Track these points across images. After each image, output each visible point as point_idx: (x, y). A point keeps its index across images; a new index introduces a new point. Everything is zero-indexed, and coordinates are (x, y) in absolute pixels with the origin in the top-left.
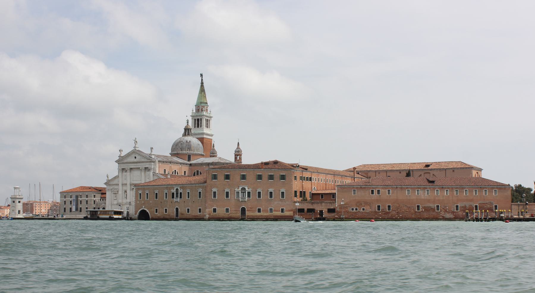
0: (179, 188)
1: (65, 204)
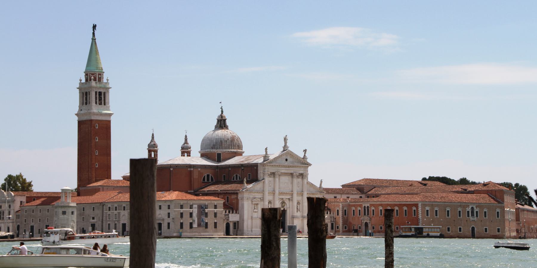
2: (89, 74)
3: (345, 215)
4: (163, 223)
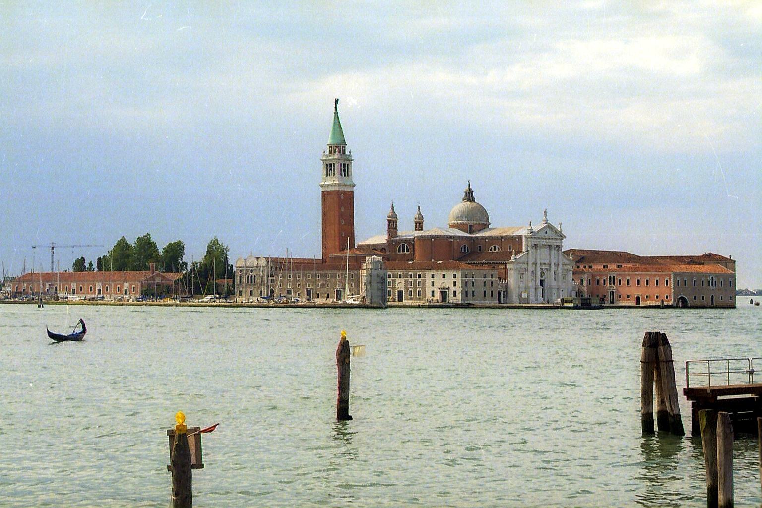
0: (714, 277)
1: (466, 286)
3: (590, 284)
4: (449, 291)
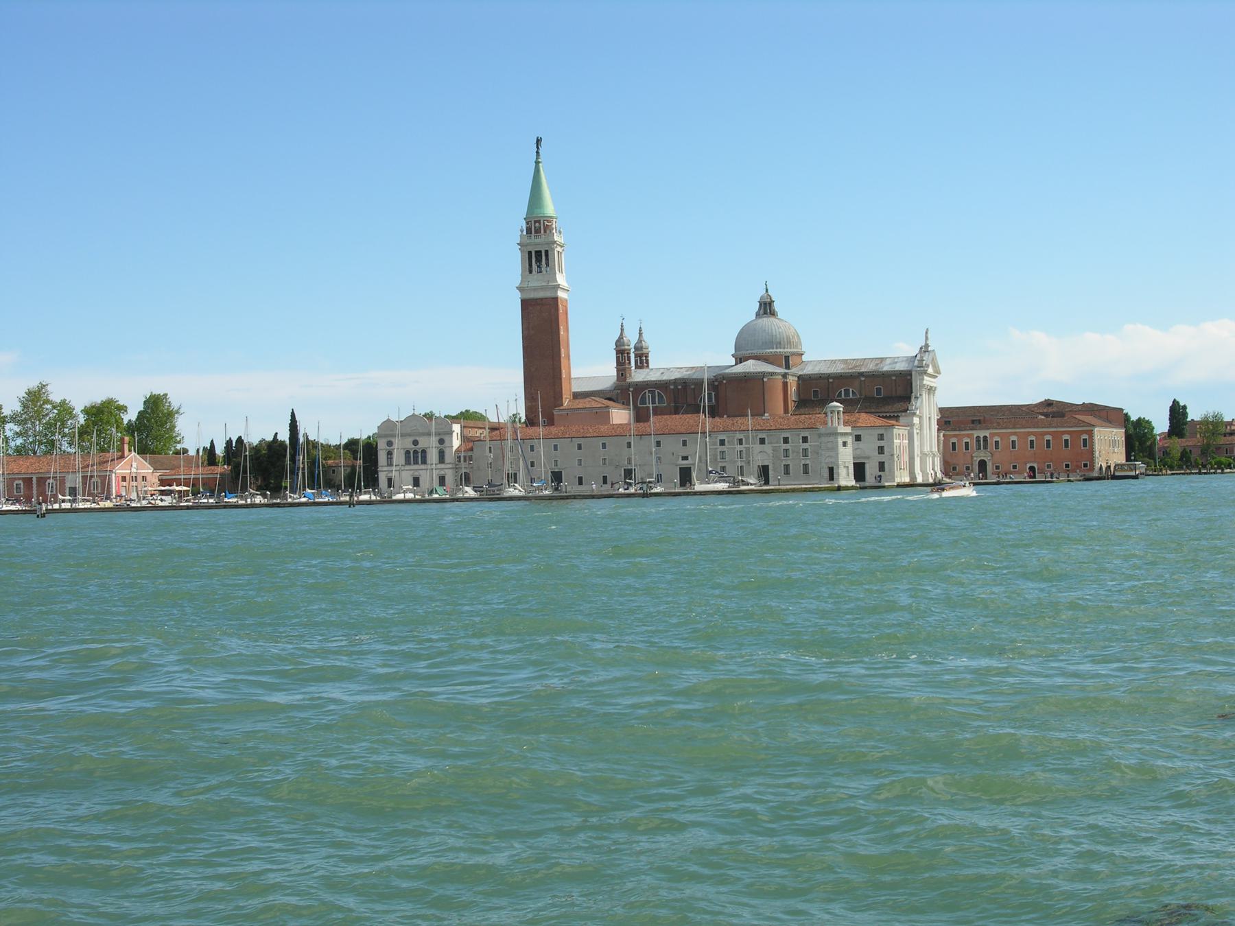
2: (542, 221)
